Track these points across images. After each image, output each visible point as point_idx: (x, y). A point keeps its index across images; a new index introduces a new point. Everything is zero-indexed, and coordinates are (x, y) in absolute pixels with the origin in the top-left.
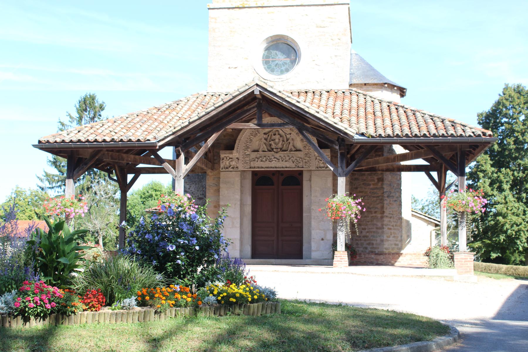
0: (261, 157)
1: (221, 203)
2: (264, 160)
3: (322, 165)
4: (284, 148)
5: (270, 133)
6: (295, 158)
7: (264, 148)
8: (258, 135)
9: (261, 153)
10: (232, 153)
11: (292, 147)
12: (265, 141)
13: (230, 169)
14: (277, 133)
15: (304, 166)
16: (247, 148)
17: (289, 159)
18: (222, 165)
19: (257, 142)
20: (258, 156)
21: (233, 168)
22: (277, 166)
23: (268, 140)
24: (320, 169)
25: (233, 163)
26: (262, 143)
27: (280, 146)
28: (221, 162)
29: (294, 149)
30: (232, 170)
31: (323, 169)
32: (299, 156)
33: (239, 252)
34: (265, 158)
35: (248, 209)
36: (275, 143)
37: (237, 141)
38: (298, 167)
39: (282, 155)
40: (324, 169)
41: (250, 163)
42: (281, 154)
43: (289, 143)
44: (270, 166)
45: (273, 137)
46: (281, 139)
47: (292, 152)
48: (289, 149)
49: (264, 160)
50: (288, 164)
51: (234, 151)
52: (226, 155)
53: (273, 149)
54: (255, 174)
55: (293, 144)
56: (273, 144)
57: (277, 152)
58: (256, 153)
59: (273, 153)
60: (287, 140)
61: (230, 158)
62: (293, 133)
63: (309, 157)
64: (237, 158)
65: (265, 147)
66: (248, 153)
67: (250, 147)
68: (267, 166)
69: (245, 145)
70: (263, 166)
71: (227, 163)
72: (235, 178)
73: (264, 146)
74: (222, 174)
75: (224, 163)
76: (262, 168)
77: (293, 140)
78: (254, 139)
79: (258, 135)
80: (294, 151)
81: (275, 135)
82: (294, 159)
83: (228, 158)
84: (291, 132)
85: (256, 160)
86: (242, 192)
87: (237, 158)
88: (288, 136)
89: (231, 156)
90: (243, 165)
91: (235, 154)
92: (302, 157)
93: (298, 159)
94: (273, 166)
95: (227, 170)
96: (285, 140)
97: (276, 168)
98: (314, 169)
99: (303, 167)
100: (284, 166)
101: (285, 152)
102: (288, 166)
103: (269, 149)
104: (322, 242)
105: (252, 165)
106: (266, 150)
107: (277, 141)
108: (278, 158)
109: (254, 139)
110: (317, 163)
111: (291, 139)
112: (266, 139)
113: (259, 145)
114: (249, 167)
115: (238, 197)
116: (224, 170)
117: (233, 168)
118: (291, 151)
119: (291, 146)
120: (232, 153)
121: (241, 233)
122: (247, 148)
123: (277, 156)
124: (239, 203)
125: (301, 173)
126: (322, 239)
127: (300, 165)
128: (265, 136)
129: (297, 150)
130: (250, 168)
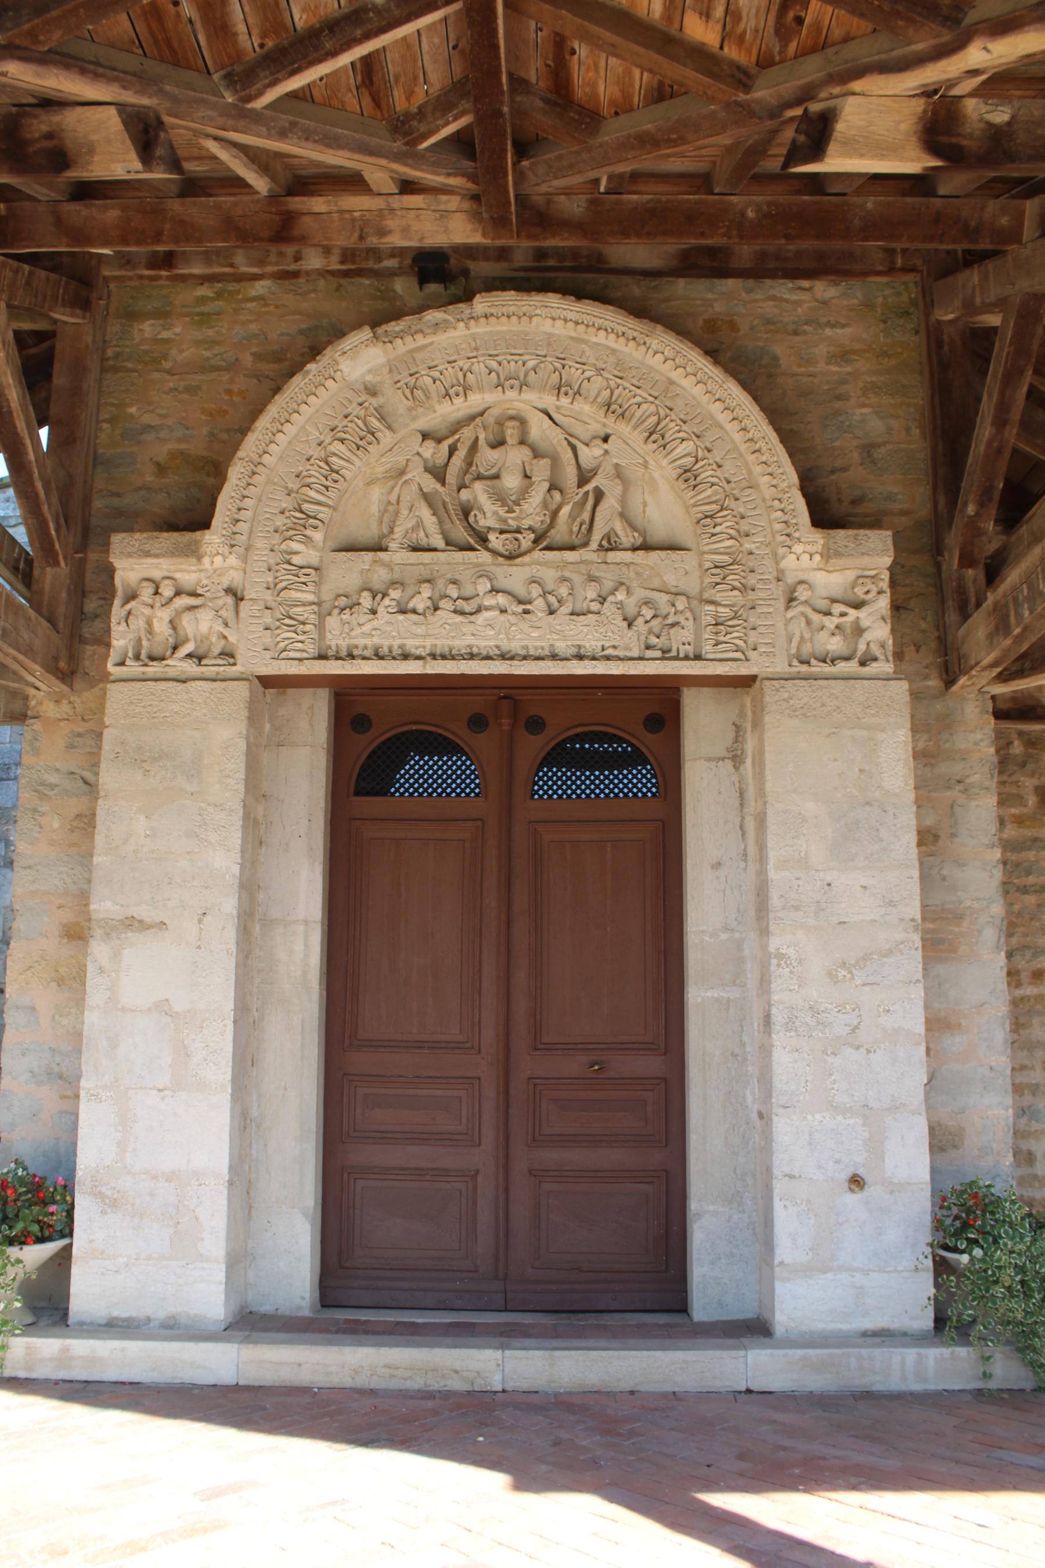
0: (394, 583)
1: (104, 905)
2: (420, 603)
3: (836, 645)
4: (560, 533)
5: (467, 434)
6: (640, 593)
7: (419, 524)
8: (387, 438)
9: (398, 556)
10: (194, 552)
11: (618, 526)
12: (430, 484)
13: (178, 665)
14: (511, 432)
15: (707, 649)
16: (302, 520)
17: (602, 600)
18: (121, 640)
19: (376, 494)
20: (380, 576)
21: (197, 657)
22: (515, 646)
23: (451, 478)
24: (818, 668)
25: (202, 625)
26: (410, 495)
27: (532, 512)
28: (117, 611)
29: (627, 538)
30: (190, 668)
31: (842, 667)
32: (671, 580)
33: (219, 1273)
34: (426, 591)
35: (300, 950)
36: (500, 498)
37: (235, 473)
38: (666, 654)
39: (549, 576)
40: (851, 667)
41: (321, 627)
42: (543, 565)
43: (599, 495)
44: (460, 644)
45: (488, 457)
46: (541, 470)
47: (611, 556)
48: (596, 537)
49: (420, 603)
50: (589, 634)
51: (212, 539)
52: (158, 567)
53: (484, 540)
54: (355, 706)
55: (623, 502)
56: (484, 500)
57: (510, 557)
58: (368, 556)
59: (484, 556)
60: (582, 481)
61: (178, 593)
62: (624, 429)
63: (744, 589)
64: (230, 591)
65: (430, 521)
66: (306, 555)
67: (324, 513)
68: (442, 644)
69: (287, 503)
70: (412, 645)
71: (162, 628)
72: (212, 726)
73: (425, 513)
74: (117, 696)
75: (138, 623)
76: (406, 656)
77: (619, 473)
78: (356, 468)
79: (387, 438)
80: (635, 549)
81: (498, 443)
82: (631, 605)
83: (167, 591)
84: (611, 424)
85: (366, 600)
86: (256, 833)
87: (230, 591)
88: (589, 455)
89: (188, 574)
90: (267, 639)
91: (216, 558)
92: (692, 585)
93: (662, 599)
94: (485, 643)
95: (154, 669)
96: (570, 475)
97: (505, 657)
98: (780, 666)
99: (698, 657)
100: (562, 647)
101: (570, 556)
102: (591, 644)
103: (460, 533)
104: (851, 1200)
105: (336, 636)
106: (440, 543)
107: (511, 482)
108: (521, 592)
109: (356, 468)
110: (798, 627)
111: (607, 468)
112: (439, 474)
113: (391, 510)
114: (312, 650)
115: (225, 860)
116: (133, 668)
117: (197, 657)
118: (610, 545)
119: (607, 520)
120: (194, 552)
121: (246, 1125)
122: (302, 520)
123: (515, 577)
124: (230, 905)
125: (657, 707)
126: (856, 1182)
127: (681, 639)
128: (428, 450)
129: (646, 547)
130: (322, 657)
